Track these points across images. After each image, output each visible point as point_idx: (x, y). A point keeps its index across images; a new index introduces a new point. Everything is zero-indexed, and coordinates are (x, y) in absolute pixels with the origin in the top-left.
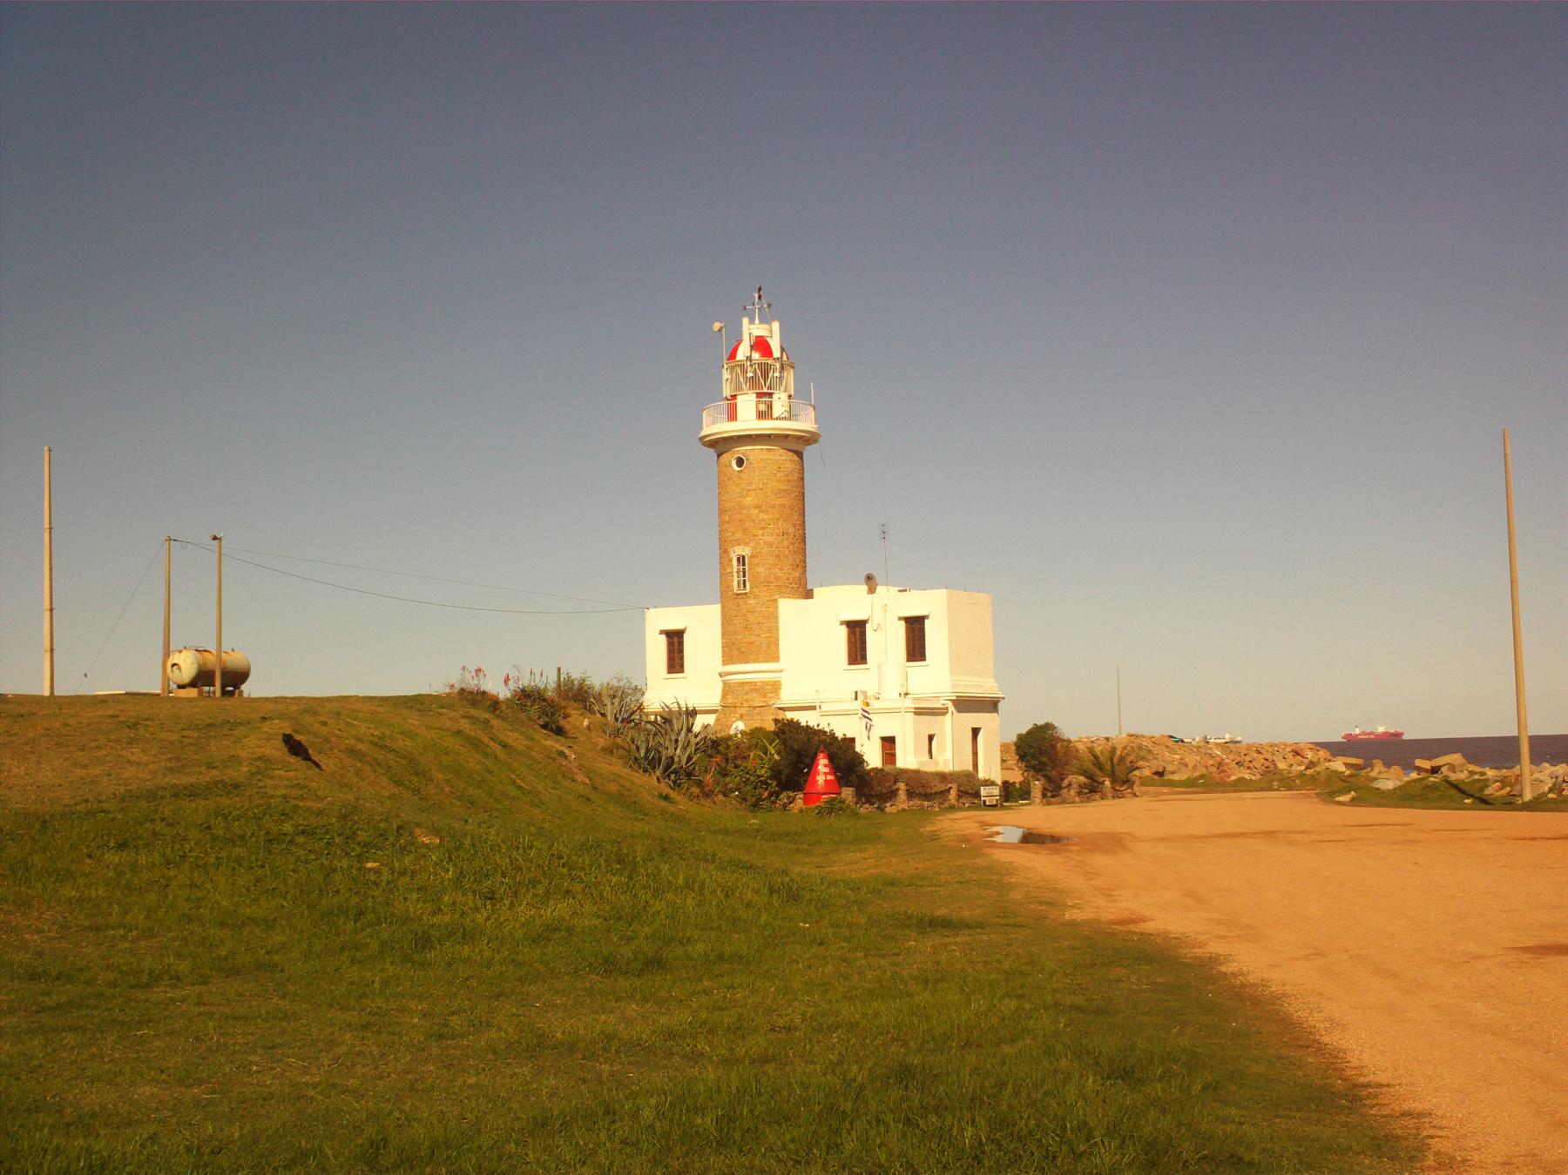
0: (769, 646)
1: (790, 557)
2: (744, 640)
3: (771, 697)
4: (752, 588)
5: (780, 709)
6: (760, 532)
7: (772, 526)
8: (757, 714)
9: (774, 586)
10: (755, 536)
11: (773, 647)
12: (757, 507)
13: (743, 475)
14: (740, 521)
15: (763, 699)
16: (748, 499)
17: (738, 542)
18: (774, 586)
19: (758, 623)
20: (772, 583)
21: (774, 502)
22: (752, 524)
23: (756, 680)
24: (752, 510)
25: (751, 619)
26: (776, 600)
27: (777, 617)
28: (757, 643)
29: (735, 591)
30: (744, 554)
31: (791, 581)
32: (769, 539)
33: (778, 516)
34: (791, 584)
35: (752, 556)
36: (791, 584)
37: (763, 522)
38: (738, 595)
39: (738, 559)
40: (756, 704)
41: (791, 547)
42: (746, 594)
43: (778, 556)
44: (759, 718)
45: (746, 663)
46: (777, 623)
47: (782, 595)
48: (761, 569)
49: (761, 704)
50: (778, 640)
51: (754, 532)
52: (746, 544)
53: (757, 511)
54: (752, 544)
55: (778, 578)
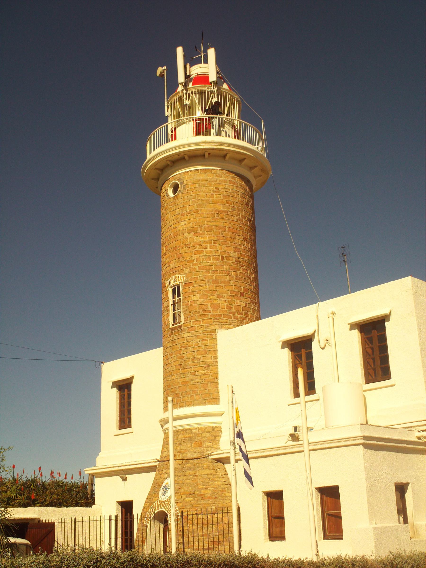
0: (205, 385)
1: (231, 283)
2: (179, 380)
3: (208, 447)
4: (186, 319)
5: (218, 460)
6: (195, 257)
7: (208, 249)
8: (190, 468)
9: (212, 315)
10: (189, 261)
11: (210, 386)
12: (192, 230)
13: (178, 201)
14: (175, 248)
15: (198, 449)
16: (182, 223)
17: (173, 272)
18: (212, 315)
19: (193, 359)
20: (209, 311)
21: (211, 224)
22: (186, 250)
23: (191, 427)
24: (186, 235)
25: (187, 355)
26: (213, 333)
27: (216, 351)
28: (192, 382)
29: (171, 326)
30: (178, 283)
31: (233, 310)
32: (205, 263)
33: (215, 238)
34: (234, 313)
35: (187, 284)
36: (234, 313)
37: (198, 246)
38: (173, 329)
39: (174, 290)
40: (190, 455)
41: (232, 273)
42: (180, 327)
43: (215, 282)
44: (192, 472)
45: (180, 407)
46: (216, 357)
47: (222, 325)
48: (195, 298)
49: (195, 456)
50: (217, 378)
51: (189, 258)
52: (180, 272)
53: (191, 235)
54: (186, 271)
55: (216, 307)
